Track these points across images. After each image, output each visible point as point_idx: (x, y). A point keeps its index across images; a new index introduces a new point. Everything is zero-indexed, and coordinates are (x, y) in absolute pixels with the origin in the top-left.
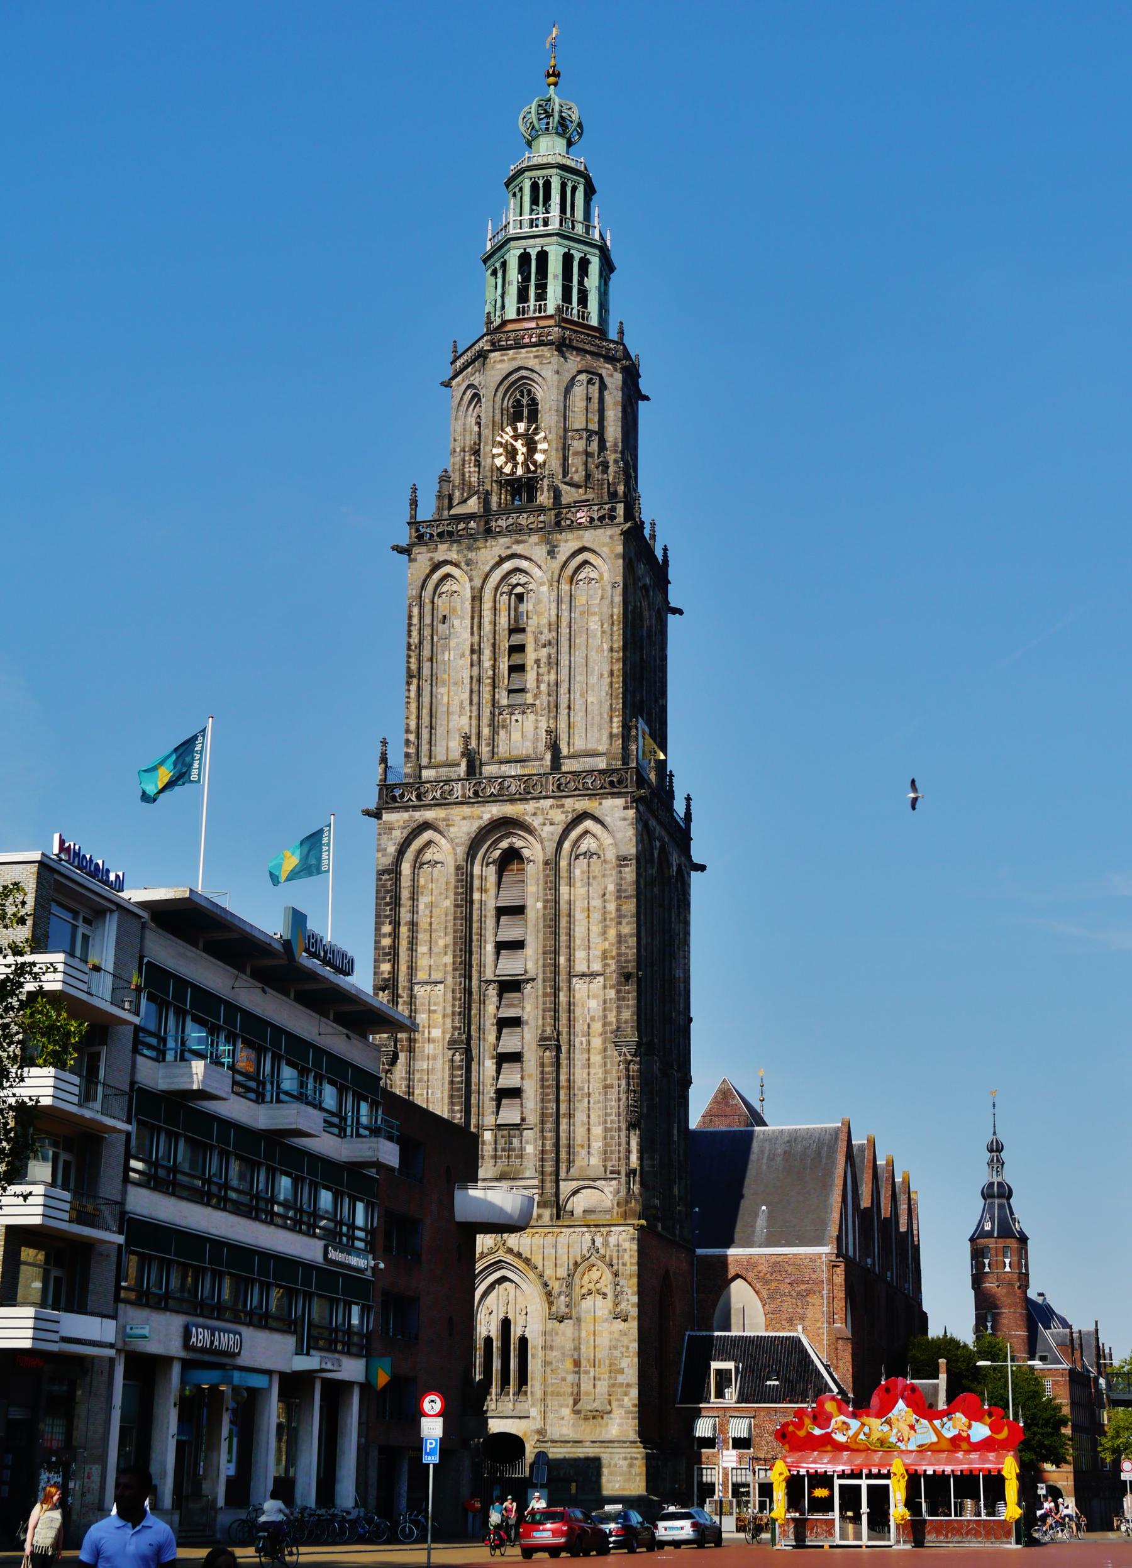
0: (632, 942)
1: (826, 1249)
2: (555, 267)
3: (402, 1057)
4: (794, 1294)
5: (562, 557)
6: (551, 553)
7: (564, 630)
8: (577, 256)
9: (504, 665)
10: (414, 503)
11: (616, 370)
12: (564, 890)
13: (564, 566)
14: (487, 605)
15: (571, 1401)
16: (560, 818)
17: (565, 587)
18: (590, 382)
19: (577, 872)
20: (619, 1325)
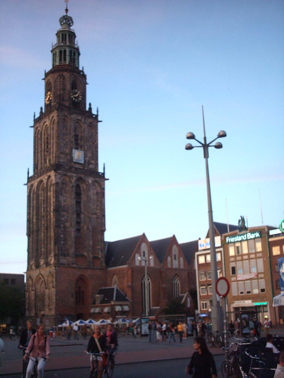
0: (55, 203)
1: (126, 266)
2: (58, 54)
3: (31, 235)
5: (50, 119)
6: (49, 119)
7: (52, 136)
8: (63, 50)
9: (46, 146)
10: (34, 116)
12: (49, 193)
13: (51, 121)
14: (43, 134)
16: (46, 177)
17: (52, 126)
18: (61, 78)
19: (52, 189)
20: (53, 289)
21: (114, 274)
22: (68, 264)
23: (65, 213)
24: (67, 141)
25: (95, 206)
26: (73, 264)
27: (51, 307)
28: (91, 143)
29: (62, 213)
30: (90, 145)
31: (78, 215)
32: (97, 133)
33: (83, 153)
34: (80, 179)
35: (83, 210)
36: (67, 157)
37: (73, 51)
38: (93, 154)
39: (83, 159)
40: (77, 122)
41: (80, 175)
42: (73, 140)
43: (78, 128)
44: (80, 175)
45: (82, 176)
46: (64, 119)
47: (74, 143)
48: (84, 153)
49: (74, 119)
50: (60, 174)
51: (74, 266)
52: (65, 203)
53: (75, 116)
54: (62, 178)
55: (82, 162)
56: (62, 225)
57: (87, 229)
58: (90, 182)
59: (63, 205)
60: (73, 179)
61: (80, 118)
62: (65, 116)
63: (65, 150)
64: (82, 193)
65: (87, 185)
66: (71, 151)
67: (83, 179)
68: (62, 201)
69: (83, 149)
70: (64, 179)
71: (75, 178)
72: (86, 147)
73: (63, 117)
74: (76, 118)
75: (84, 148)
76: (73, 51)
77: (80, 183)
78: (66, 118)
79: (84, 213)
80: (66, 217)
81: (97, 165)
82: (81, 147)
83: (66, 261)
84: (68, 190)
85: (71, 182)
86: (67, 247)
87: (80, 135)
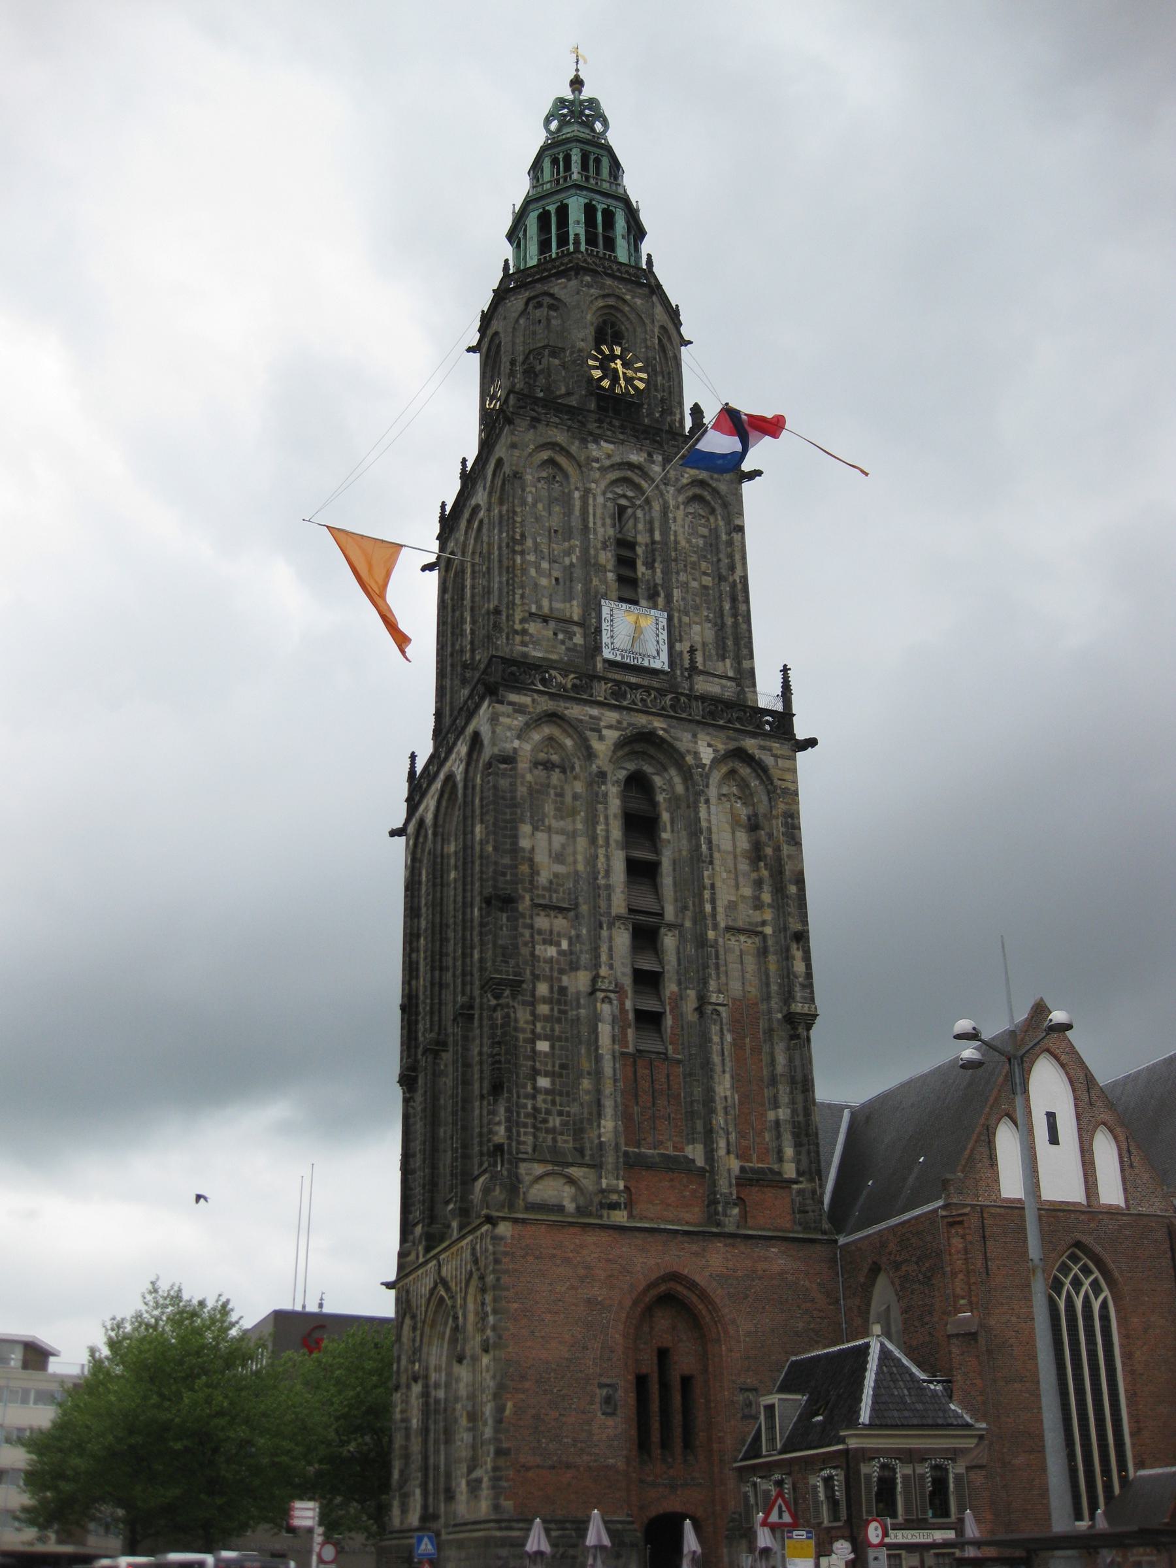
4: (921, 1277)
8: (552, 208)
11: (569, 280)
15: (465, 1470)
21: (875, 1270)
22: (580, 1211)
23: (560, 923)
24: (572, 565)
25: (747, 891)
26: (614, 1206)
27: (478, 1473)
28: (707, 581)
29: (542, 922)
30: (706, 587)
31: (646, 936)
32: (740, 529)
33: (663, 622)
34: (640, 743)
35: (670, 913)
36: (570, 636)
37: (600, 207)
38: (720, 627)
39: (665, 648)
40: (625, 480)
41: (642, 720)
42: (606, 558)
43: (630, 511)
44: (642, 720)
45: (658, 724)
46: (551, 462)
47: (611, 576)
48: (670, 619)
49: (607, 463)
50: (520, 709)
51: (620, 1217)
52: (560, 869)
53: (608, 447)
54: (536, 737)
55: (661, 662)
56: (543, 989)
57: (700, 1010)
58: (707, 755)
59: (543, 879)
60: (601, 738)
61: (635, 458)
62: (553, 445)
63: (557, 605)
64: (665, 816)
65: (687, 774)
66: (592, 606)
67: (663, 740)
68: (541, 858)
69: (661, 601)
70: (551, 739)
71: (612, 735)
72: (677, 593)
73: (545, 455)
74: (617, 459)
75: (669, 598)
76: (600, 207)
77: (648, 769)
78: (562, 460)
79: (682, 925)
80: (565, 945)
81: (746, 677)
82: (652, 597)
83: (568, 1191)
84: (575, 797)
85: (590, 755)
86: (574, 1109)
87: (642, 539)
